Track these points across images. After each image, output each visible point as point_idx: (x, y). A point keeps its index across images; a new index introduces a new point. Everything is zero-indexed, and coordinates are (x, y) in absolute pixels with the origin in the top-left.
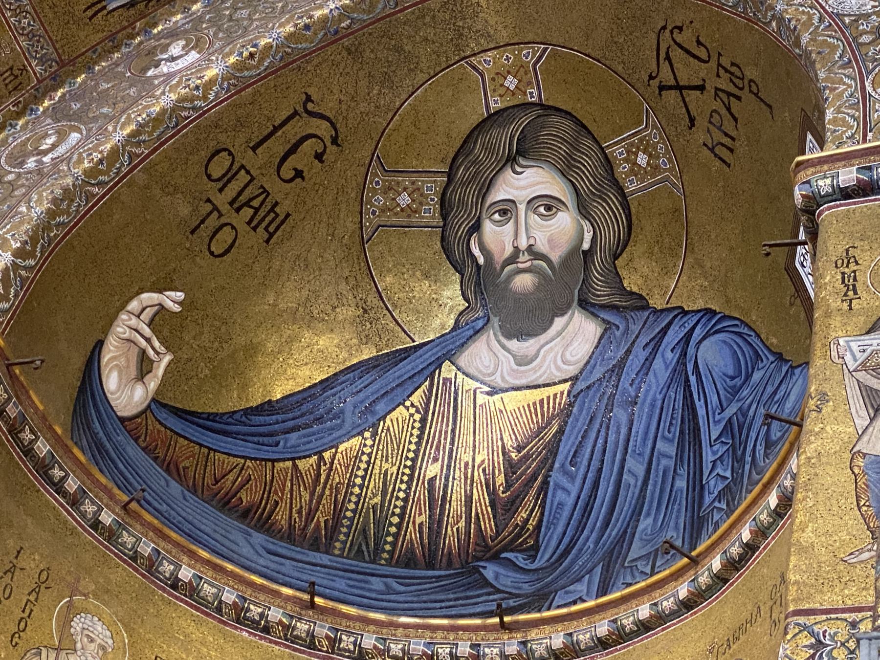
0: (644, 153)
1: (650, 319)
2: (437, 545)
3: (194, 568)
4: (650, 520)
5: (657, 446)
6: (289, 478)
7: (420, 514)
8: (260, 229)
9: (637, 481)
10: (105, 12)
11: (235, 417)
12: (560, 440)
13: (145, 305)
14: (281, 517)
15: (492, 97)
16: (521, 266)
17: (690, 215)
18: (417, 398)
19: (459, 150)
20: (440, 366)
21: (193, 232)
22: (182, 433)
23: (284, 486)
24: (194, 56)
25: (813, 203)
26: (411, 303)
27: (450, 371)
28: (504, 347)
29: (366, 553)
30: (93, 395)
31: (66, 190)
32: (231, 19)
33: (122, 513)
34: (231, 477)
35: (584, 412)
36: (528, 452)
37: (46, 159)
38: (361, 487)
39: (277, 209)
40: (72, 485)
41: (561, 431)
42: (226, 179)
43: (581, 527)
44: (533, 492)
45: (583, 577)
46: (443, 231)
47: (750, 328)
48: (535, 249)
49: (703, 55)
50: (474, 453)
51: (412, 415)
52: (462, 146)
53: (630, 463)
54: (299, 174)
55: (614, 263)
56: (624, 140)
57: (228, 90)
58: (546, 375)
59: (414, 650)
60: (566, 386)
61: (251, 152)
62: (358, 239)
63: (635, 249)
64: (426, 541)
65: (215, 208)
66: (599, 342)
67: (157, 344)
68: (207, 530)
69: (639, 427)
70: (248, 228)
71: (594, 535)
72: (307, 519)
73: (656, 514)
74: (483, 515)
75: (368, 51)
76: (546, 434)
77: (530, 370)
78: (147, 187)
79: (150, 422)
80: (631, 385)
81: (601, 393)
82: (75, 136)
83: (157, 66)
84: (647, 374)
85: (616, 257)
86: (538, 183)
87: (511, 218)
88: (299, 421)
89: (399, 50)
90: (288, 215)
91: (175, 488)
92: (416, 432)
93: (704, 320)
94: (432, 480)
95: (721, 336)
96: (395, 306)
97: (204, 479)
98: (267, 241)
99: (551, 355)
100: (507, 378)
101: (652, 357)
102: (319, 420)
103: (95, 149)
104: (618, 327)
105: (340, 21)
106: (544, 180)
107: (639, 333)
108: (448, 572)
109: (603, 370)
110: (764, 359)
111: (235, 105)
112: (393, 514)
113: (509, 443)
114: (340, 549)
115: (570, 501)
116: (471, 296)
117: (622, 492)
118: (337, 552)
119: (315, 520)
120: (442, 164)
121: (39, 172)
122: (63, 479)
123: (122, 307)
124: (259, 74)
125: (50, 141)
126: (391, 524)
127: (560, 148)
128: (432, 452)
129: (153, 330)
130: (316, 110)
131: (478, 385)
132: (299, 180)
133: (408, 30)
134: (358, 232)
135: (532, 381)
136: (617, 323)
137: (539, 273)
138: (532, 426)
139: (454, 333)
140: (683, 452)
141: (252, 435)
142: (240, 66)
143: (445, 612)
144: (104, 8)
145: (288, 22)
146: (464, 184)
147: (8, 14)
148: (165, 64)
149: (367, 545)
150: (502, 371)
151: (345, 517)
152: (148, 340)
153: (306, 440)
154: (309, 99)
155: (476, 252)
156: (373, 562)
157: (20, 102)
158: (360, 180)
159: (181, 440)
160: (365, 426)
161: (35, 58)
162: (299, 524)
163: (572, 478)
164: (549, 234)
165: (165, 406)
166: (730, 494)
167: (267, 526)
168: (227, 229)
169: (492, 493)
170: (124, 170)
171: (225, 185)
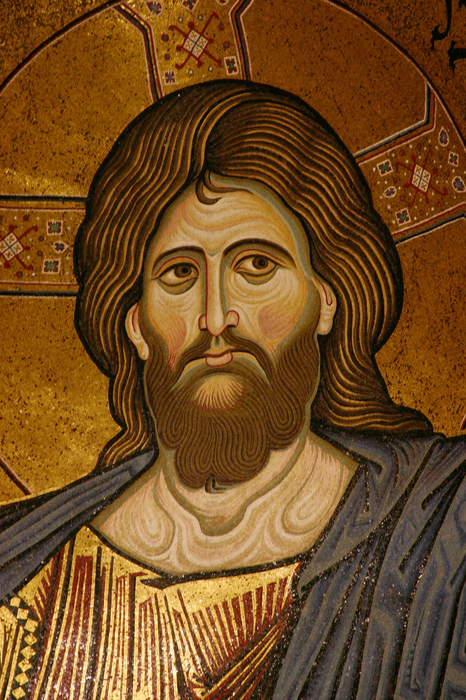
0: (424, 168)
1: (434, 455)
5: (447, 677)
12: (280, 666)
15: (162, 69)
16: (212, 361)
19: (107, 160)
20: (72, 537)
26: (22, 425)
28: (183, 502)
35: (321, 616)
36: (224, 686)
46: (78, 301)
50: (130, 690)
51: (22, 623)
52: (111, 154)
55: (372, 357)
56: (388, 145)
58: (256, 551)
66: (346, 494)
76: (255, 654)
77: (228, 542)
80: (402, 568)
81: (349, 583)
84: (429, 550)
86: (243, 220)
87: (196, 279)
92: (28, 652)
99: (265, 516)
100: (189, 556)
101: (437, 519)
104: (379, 469)
106: (253, 213)
107: (416, 479)
109: (354, 542)
116: (128, 415)
120: (76, 186)
127: (280, 158)
128: (57, 687)
131: (136, 569)
135: (231, 562)
136: (377, 460)
137: (243, 374)
138: (230, 640)
139: (98, 479)
146: (115, 220)
150: (180, 544)
164: (261, 307)
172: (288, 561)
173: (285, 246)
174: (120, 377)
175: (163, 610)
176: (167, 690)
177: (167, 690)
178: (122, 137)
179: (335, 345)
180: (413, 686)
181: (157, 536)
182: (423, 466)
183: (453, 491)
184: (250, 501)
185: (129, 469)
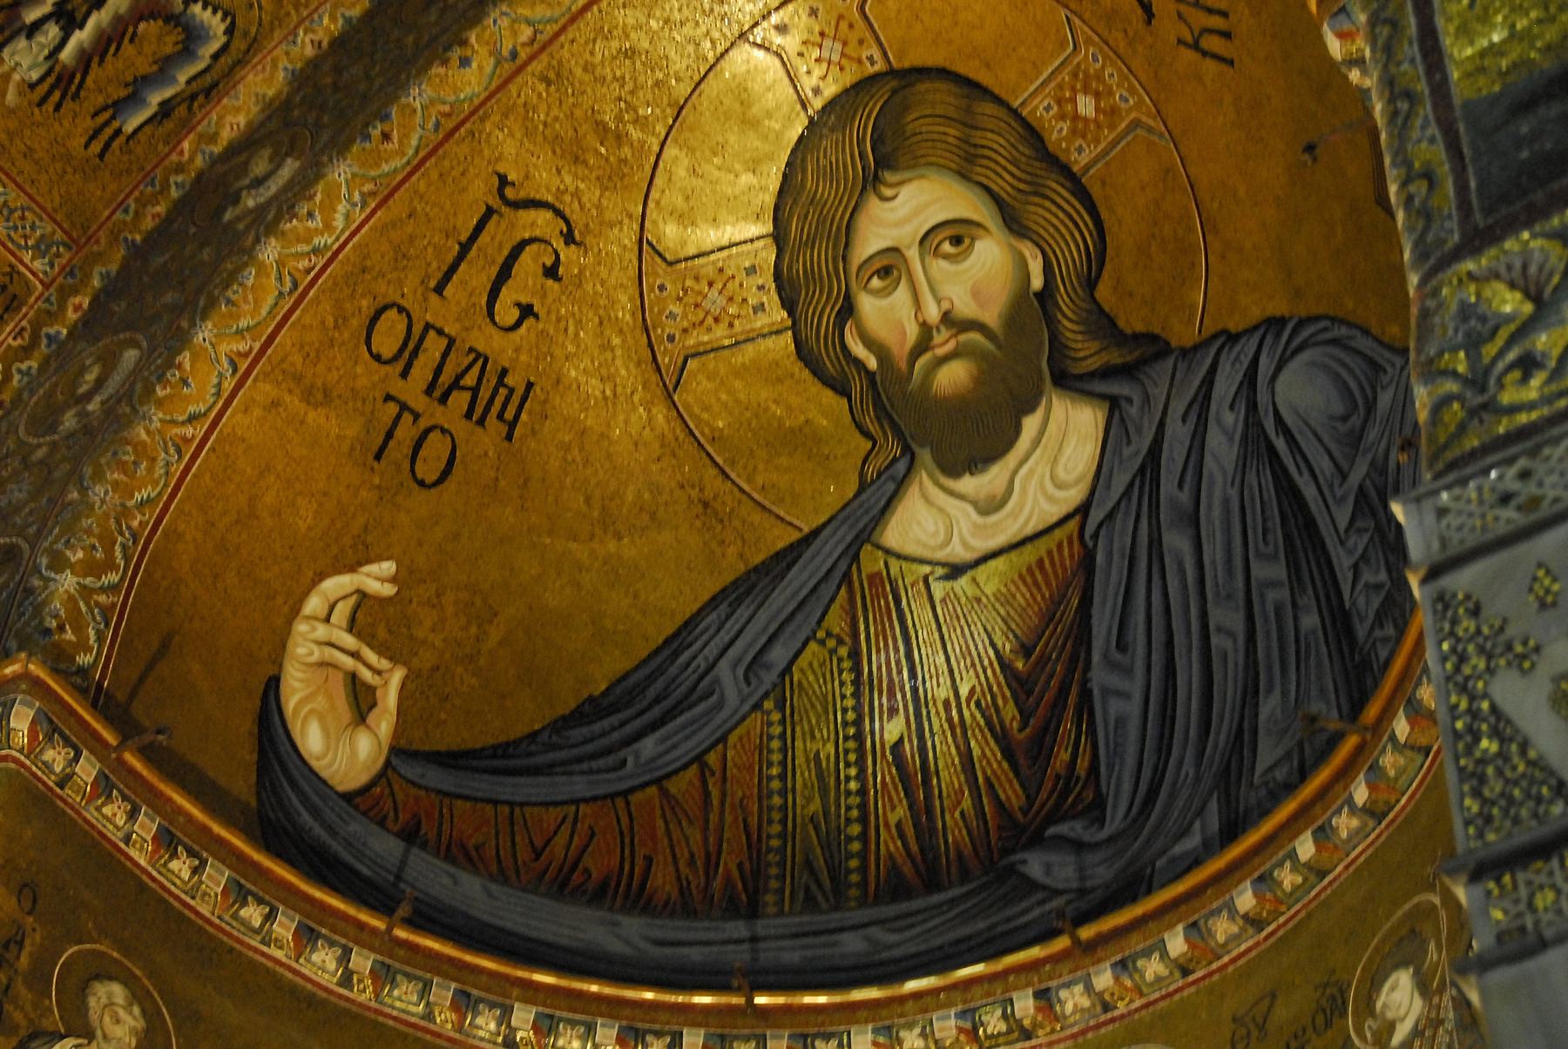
3: (535, 1004)
6: (658, 812)
7: (893, 808)
9: (1235, 640)
10: (121, 139)
11: (539, 739)
13: (332, 600)
14: (662, 881)
16: (940, 352)
17: (1192, 170)
18: (836, 621)
19: (781, 192)
20: (856, 558)
21: (378, 457)
22: (459, 791)
23: (654, 828)
24: (289, 168)
27: (876, 560)
29: (819, 897)
30: (285, 770)
34: (560, 840)
37: (90, 407)
42: (406, 354)
45: (1191, 823)
47: (1350, 325)
48: (952, 315)
51: (833, 652)
53: (1216, 616)
54: (527, 311)
57: (364, 204)
59: (941, 1030)
60: (1073, 525)
61: (434, 298)
62: (659, 392)
64: (915, 848)
65: (404, 407)
67: (371, 656)
69: (1213, 552)
70: (470, 425)
72: (707, 874)
73: (1283, 685)
74: (998, 779)
75: (578, 72)
77: (1008, 515)
79: (396, 788)
80: (1180, 486)
82: (131, 355)
83: (236, 199)
85: (1091, 283)
86: (927, 205)
87: (900, 278)
89: (631, 53)
90: (530, 385)
93: (1269, 340)
95: (1305, 356)
97: (514, 855)
98: (509, 437)
99: (1036, 479)
101: (1201, 428)
104: (1130, 401)
105: (515, 34)
108: (964, 889)
110: (1389, 369)
111: (384, 228)
112: (848, 821)
114: (776, 904)
115: (1134, 708)
118: (771, 910)
119: (721, 870)
120: (759, 225)
121: (87, 430)
123: (295, 611)
124: (408, 163)
125: (91, 377)
126: (849, 839)
129: (359, 636)
130: (522, 194)
131: (927, 569)
134: (655, 378)
139: (864, 496)
140: (1298, 570)
141: (579, 760)
148: (249, 194)
149: (820, 886)
151: (769, 850)
152: (355, 655)
153: (669, 743)
154: (503, 181)
155: (859, 350)
156: (837, 908)
157: (23, 329)
160: (761, 692)
161: (27, 247)
163: (1127, 671)
167: (642, 902)
168: (434, 436)
169: (1002, 737)
170: (228, 385)
171: (409, 366)
173: (975, 217)
175: (963, 600)
176: (989, 672)
177: (989, 672)
179: (1053, 297)
180: (1223, 593)
181: (937, 532)
182: (1171, 385)
183: (1208, 397)
184: (1015, 472)
185: (892, 478)
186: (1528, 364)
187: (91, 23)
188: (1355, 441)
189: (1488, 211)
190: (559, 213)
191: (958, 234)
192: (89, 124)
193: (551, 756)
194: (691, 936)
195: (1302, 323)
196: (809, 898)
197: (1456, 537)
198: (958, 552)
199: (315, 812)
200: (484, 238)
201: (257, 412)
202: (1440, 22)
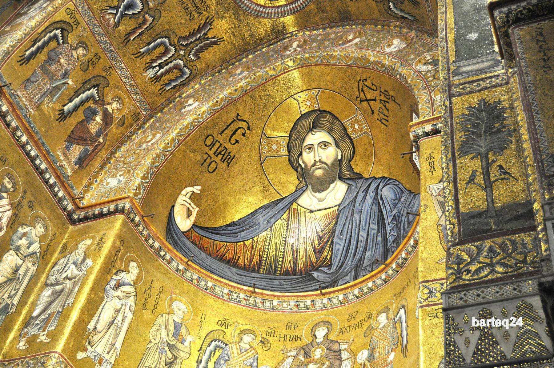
2: (296, 267)
4: (370, 252)
8: (225, 162)
14: (241, 262)
16: (317, 167)
18: (285, 216)
20: (292, 204)
21: (202, 165)
24: (197, 103)
25: (417, 137)
28: (314, 196)
30: (172, 226)
31: (157, 154)
32: (209, 90)
33: (186, 265)
34: (222, 249)
38: (268, 249)
39: (231, 154)
40: (168, 257)
41: (336, 224)
43: (346, 256)
44: (328, 246)
49: (374, 88)
54: (237, 141)
60: (337, 208)
61: (219, 135)
63: (357, 158)
65: (209, 156)
68: (216, 268)
69: (363, 220)
71: (351, 259)
78: (185, 151)
82: (158, 136)
83: (185, 108)
85: (350, 161)
88: (244, 228)
89: (268, 95)
90: (234, 156)
91: (203, 255)
92: (286, 228)
94: (293, 244)
95: (389, 186)
96: (274, 184)
98: (228, 166)
102: (251, 227)
103: (166, 139)
105: (247, 87)
113: (319, 229)
115: (341, 248)
116: (301, 179)
117: (359, 243)
121: (147, 149)
122: (165, 255)
123: (180, 193)
126: (279, 261)
129: (191, 200)
132: (237, 144)
133: (270, 88)
142: (214, 106)
143: (301, 290)
144: (165, 90)
145: (229, 89)
147: (132, 95)
152: (189, 204)
154: (238, 115)
156: (274, 275)
158: (259, 141)
159: (204, 238)
162: (247, 263)
163: (341, 239)
165: (197, 226)
166: (397, 242)
169: (314, 247)
170: (176, 145)
171: (212, 148)
172: (336, 206)
174: (299, 172)
178: (295, 123)
186: (468, 271)
187: (165, 68)
188: (395, 205)
189: (464, 237)
190: (248, 123)
191: (325, 145)
192: (159, 87)
193: (224, 232)
194: (245, 274)
195: (390, 179)
196: (269, 271)
197: (452, 303)
198: (313, 208)
199: (177, 235)
200: (232, 125)
201: (181, 152)
202: (459, 194)
